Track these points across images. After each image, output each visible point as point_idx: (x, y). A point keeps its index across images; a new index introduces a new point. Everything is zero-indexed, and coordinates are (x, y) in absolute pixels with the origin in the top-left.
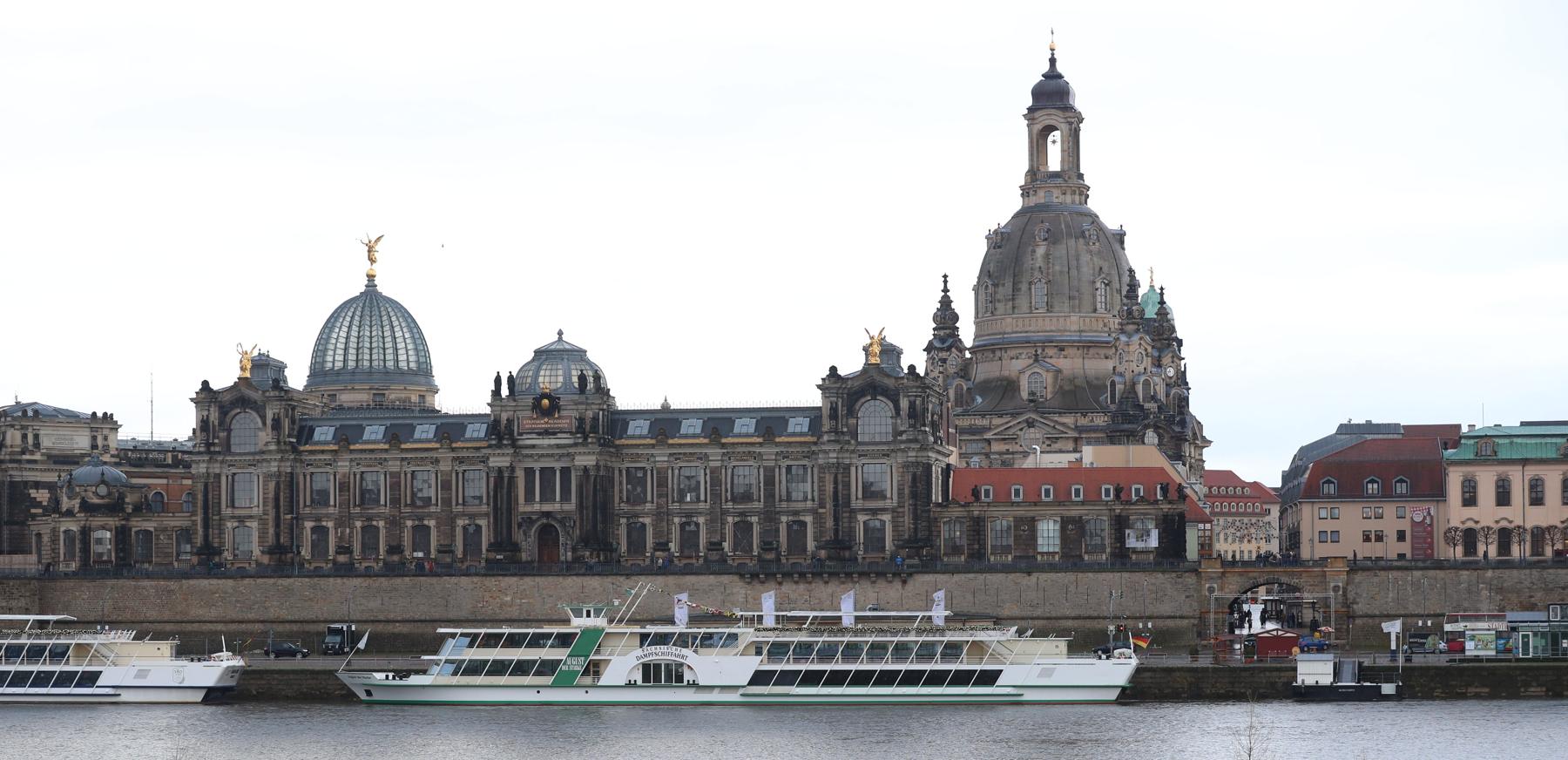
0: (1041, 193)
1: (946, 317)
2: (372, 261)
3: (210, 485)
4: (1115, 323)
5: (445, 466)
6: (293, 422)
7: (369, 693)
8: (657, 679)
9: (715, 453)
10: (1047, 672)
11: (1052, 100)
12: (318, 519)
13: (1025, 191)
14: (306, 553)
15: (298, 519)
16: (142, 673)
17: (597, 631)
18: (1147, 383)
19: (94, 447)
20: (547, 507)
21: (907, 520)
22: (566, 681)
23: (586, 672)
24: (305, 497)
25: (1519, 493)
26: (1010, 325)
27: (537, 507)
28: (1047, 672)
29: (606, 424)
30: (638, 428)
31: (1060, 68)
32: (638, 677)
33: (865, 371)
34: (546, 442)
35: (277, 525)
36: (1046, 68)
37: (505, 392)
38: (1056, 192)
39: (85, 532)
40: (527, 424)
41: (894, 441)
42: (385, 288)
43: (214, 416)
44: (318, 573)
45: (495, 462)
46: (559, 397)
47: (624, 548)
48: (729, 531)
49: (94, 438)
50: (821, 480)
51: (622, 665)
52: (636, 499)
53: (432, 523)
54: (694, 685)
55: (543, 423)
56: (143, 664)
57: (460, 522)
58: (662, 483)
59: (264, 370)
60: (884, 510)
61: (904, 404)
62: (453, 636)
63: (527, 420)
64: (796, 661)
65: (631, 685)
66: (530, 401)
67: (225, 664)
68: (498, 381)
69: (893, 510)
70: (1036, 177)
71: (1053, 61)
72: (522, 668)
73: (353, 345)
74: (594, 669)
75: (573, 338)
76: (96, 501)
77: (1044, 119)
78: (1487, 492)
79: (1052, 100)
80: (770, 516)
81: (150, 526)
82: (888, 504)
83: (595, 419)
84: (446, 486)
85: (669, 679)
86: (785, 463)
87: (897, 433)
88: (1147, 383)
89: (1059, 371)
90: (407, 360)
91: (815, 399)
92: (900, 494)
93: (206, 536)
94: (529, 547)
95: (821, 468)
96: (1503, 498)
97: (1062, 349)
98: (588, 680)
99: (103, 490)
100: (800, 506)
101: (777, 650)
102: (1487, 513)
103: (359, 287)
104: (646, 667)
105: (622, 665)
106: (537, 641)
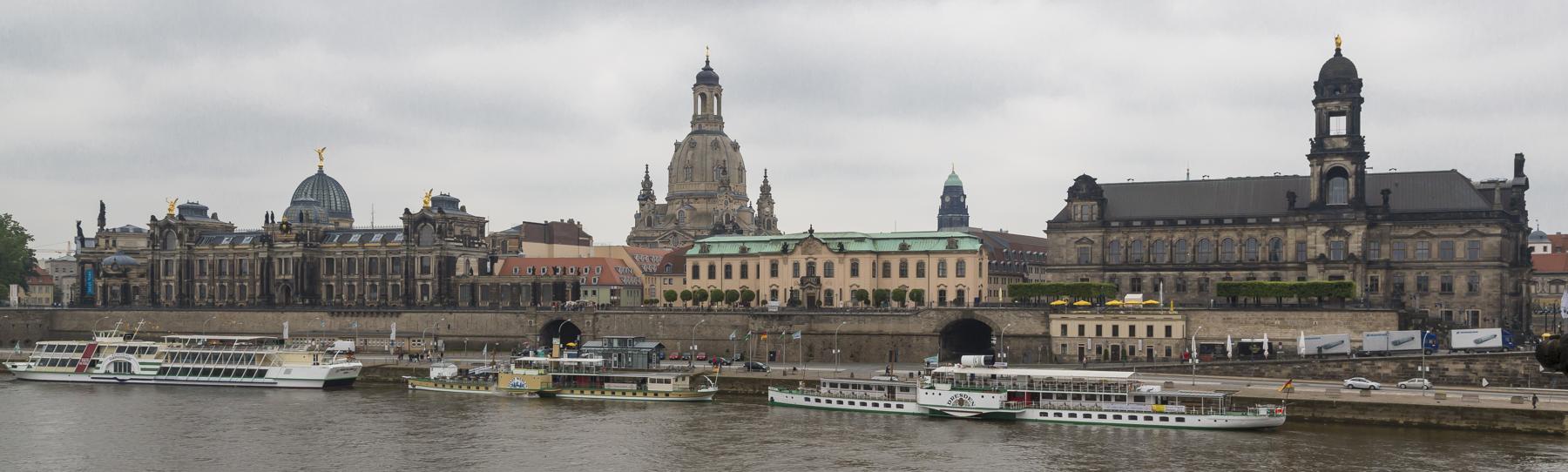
1: (647, 184)
6: (191, 235)
10: (288, 372)
11: (707, 80)
13: (693, 124)
14: (197, 298)
15: (193, 281)
22: (80, 370)
25: (719, 272)
26: (678, 189)
28: (288, 372)
32: (112, 369)
43: (157, 232)
44: (200, 308)
47: (324, 296)
48: (367, 289)
51: (105, 363)
52: (330, 272)
55: (284, 236)
58: (340, 265)
72: (63, 363)
74: (93, 364)
78: (704, 272)
79: (707, 80)
80: (384, 282)
91: (400, 224)
96: (712, 275)
102: (704, 283)
103: (315, 171)
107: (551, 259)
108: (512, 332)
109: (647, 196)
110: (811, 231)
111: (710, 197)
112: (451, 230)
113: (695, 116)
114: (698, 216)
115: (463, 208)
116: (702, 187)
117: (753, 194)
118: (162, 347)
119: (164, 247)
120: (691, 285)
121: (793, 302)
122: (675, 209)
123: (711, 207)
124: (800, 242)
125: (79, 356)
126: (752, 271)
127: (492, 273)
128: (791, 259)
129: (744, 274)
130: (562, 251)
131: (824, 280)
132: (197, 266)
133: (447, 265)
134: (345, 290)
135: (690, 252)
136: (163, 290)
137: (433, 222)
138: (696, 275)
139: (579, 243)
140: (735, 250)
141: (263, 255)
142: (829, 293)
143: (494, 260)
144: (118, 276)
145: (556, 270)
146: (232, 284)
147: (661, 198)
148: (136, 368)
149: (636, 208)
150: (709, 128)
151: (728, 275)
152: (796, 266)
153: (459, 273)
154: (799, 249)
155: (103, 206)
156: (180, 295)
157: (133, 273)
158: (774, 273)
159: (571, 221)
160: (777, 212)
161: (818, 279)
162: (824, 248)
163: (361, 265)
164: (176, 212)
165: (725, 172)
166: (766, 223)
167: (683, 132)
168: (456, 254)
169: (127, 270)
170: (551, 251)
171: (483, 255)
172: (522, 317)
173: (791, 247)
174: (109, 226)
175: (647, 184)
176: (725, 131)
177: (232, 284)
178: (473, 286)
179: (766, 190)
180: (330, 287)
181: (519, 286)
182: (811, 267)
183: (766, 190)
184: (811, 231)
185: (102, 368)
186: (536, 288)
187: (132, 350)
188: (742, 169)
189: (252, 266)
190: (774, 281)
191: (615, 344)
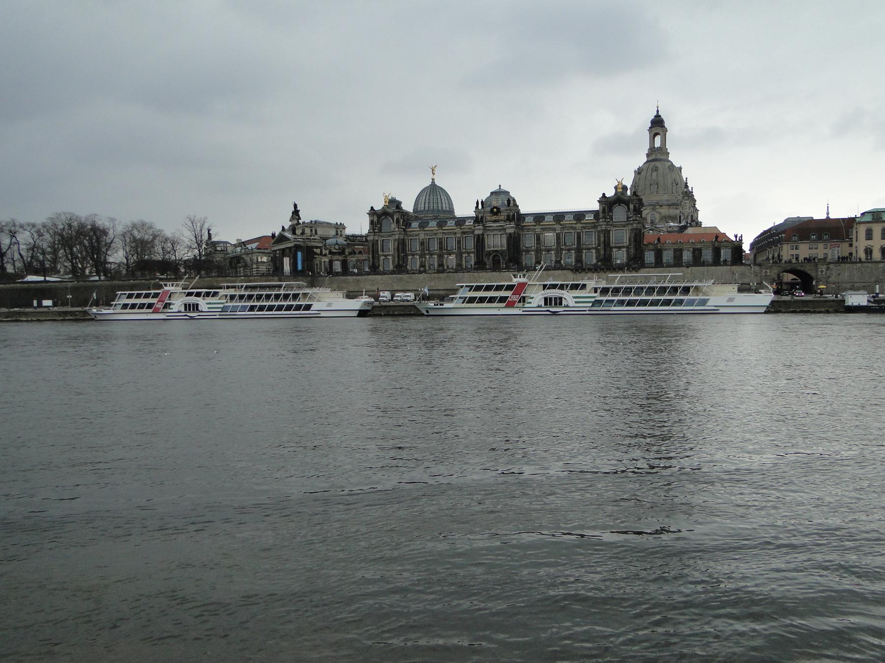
2: (433, 174)
3: (375, 243)
4: (680, 198)
7: (427, 312)
8: (551, 304)
9: (558, 227)
11: (658, 124)
12: (413, 255)
13: (648, 155)
15: (406, 255)
16: (330, 305)
17: (524, 284)
21: (632, 251)
22: (511, 305)
23: (520, 302)
29: (517, 218)
30: (529, 220)
32: (543, 303)
33: (616, 194)
37: (480, 207)
39: (331, 262)
40: (489, 218)
41: (628, 220)
43: (375, 219)
45: (476, 232)
46: (500, 209)
50: (599, 236)
51: (536, 298)
54: (567, 306)
55: (494, 218)
56: (329, 301)
59: (394, 204)
61: (631, 206)
62: (462, 287)
63: (489, 217)
64: (613, 296)
65: (539, 306)
66: (489, 209)
67: (363, 300)
68: (477, 203)
69: (627, 247)
70: (652, 150)
71: (658, 111)
72: (492, 300)
75: (503, 188)
77: (655, 130)
79: (658, 124)
82: (625, 245)
83: (514, 215)
84: (459, 242)
85: (556, 304)
86: (585, 230)
87: (628, 218)
90: (445, 207)
91: (596, 207)
92: (630, 240)
94: (489, 262)
95: (599, 232)
98: (521, 305)
99: (337, 247)
101: (605, 291)
103: (429, 183)
104: (546, 299)
105: (536, 298)
106: (499, 288)
119: (380, 231)
125: (508, 294)
141: (480, 232)
150: (662, 157)
155: (295, 206)
167: (641, 159)
169: (344, 250)
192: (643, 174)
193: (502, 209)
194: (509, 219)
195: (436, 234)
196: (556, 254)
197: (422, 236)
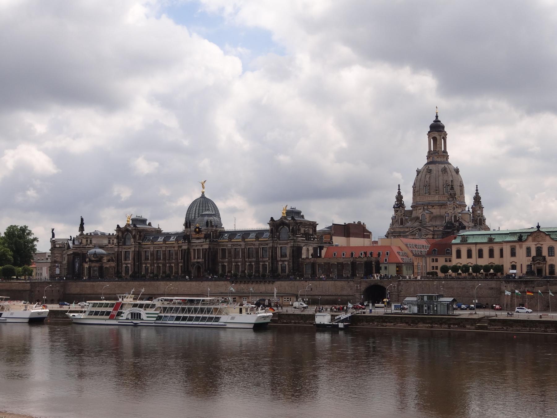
0: (431, 158)
1: (399, 198)
5: (176, 249)
6: (140, 236)
9: (243, 243)
12: (146, 264)
18: (455, 217)
19: (109, 243)
20: (199, 260)
21: (291, 264)
24: (143, 258)
25: (474, 253)
27: (196, 260)
31: (439, 119)
34: (198, 241)
35: (134, 265)
36: (435, 119)
38: (435, 158)
42: (207, 196)
43: (120, 235)
49: (109, 241)
52: (224, 257)
53: (173, 265)
55: (197, 236)
57: (180, 265)
58: (230, 253)
60: (285, 261)
61: (291, 228)
69: (288, 261)
71: (437, 117)
73: (197, 212)
76: (93, 259)
78: (464, 253)
80: (257, 263)
81: (108, 266)
82: (287, 259)
86: (261, 247)
88: (455, 217)
89: (432, 213)
91: (268, 227)
93: (118, 269)
96: (469, 255)
97: (433, 206)
100: (265, 259)
102: (464, 260)
103: (199, 195)
107: (349, 247)
108: (345, 293)
109: (399, 204)
110: (538, 227)
111: (442, 205)
112: (299, 230)
113: (430, 152)
114: (434, 218)
115: (303, 217)
116: (436, 198)
117: (469, 201)
118: (157, 302)
119: (124, 244)
120: (455, 261)
121: (530, 272)
122: (419, 213)
123: (443, 211)
124: (530, 234)
126: (497, 253)
127: (320, 256)
128: (525, 245)
129: (491, 254)
130: (356, 242)
131: (548, 258)
132: (143, 254)
133: (297, 251)
134: (233, 268)
135: (454, 241)
136: (124, 269)
137: (288, 225)
138: (459, 256)
139: (364, 237)
140: (485, 240)
141: (185, 247)
142: (552, 267)
143: (321, 248)
144: (97, 261)
145: (365, 253)
146: (164, 265)
147: (408, 207)
148: (144, 316)
149: (392, 213)
150: (439, 160)
151: (480, 255)
152: (529, 250)
153: (304, 256)
154: (530, 238)
155: (82, 220)
156: (134, 272)
157: (105, 260)
158: (513, 254)
159: (359, 223)
160: (485, 214)
161: (544, 258)
162: (548, 238)
163: (243, 252)
164: (131, 222)
165: (452, 188)
166: (479, 221)
167: (422, 161)
168: (302, 245)
169: (102, 258)
170: (348, 242)
171: (315, 246)
172: (352, 283)
173: (524, 238)
174: (85, 233)
175: (399, 198)
176: (450, 161)
177: (164, 265)
178: (313, 265)
179: (477, 199)
180: (224, 266)
181: (342, 264)
182: (539, 250)
183: (477, 199)
184: (538, 227)
185: (124, 316)
186: (354, 266)
187: (141, 306)
188: (462, 186)
189: (177, 254)
190: (513, 259)
191: (425, 299)
192: (420, 175)
193: (203, 228)
194: (207, 237)
195: (161, 248)
196: (242, 264)
197: (152, 249)
